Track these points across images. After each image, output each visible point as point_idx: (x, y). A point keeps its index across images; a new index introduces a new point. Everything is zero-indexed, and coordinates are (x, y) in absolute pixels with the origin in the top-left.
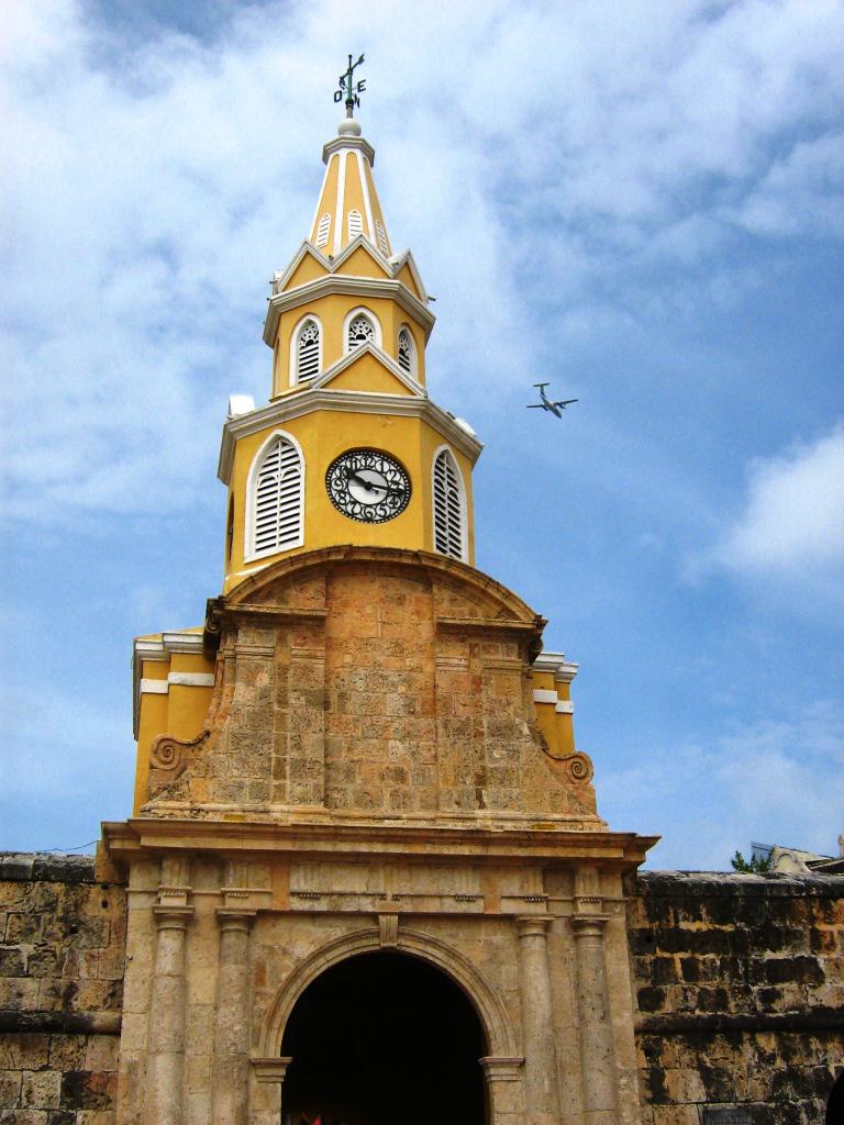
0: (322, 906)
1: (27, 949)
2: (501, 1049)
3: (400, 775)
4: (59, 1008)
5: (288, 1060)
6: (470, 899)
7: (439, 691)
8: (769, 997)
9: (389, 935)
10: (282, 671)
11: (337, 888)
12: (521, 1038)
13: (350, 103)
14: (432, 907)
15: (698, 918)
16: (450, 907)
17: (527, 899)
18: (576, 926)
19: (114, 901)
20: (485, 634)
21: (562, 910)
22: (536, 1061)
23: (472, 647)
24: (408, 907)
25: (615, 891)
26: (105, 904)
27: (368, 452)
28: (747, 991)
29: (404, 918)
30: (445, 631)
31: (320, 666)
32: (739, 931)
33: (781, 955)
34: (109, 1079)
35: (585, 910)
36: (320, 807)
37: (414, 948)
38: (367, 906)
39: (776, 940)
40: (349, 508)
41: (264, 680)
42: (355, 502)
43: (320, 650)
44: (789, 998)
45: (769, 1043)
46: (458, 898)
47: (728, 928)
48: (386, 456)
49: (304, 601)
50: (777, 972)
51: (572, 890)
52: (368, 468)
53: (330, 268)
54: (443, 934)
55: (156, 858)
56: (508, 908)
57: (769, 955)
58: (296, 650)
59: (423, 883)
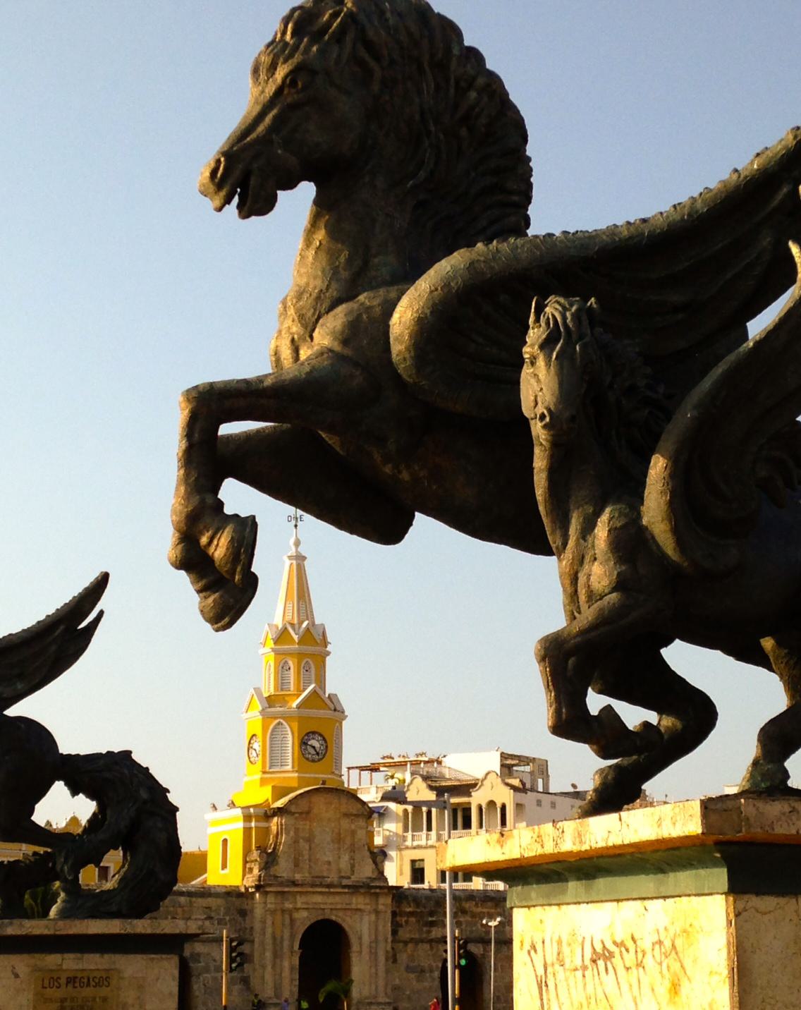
0: (311, 907)
1: (228, 918)
2: (355, 948)
3: (329, 863)
4: (237, 936)
5: (301, 951)
6: (350, 904)
7: (342, 836)
8: (429, 932)
9: (327, 917)
10: (297, 830)
11: (314, 901)
12: (361, 945)
13: (296, 526)
14: (339, 906)
15: (410, 906)
16: (344, 906)
17: (365, 904)
18: (377, 912)
19: (250, 903)
20: (357, 816)
21: (374, 907)
22: (365, 950)
23: (352, 820)
24: (333, 907)
25: (389, 900)
26: (247, 904)
27: (314, 733)
28: (422, 930)
29: (331, 909)
30: (346, 815)
31: (308, 827)
32: (421, 912)
33: (434, 919)
34: (252, 955)
35: (381, 907)
36: (307, 875)
37: (334, 918)
38: (322, 906)
39: (431, 914)
40: (307, 756)
41: (292, 833)
42: (309, 753)
43: (308, 822)
44: (434, 933)
45: (427, 946)
46: (347, 904)
47: (419, 910)
48: (321, 735)
49: (304, 806)
50: (432, 924)
51: (377, 901)
52: (313, 739)
53: (296, 637)
54: (341, 914)
55: (267, 893)
56: (359, 907)
57: (430, 919)
58: (301, 824)
59: (337, 899)
